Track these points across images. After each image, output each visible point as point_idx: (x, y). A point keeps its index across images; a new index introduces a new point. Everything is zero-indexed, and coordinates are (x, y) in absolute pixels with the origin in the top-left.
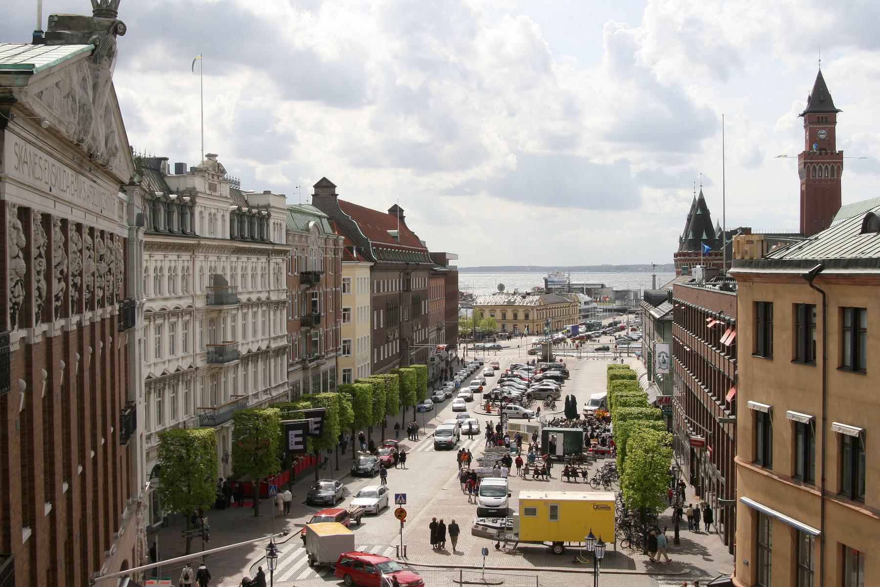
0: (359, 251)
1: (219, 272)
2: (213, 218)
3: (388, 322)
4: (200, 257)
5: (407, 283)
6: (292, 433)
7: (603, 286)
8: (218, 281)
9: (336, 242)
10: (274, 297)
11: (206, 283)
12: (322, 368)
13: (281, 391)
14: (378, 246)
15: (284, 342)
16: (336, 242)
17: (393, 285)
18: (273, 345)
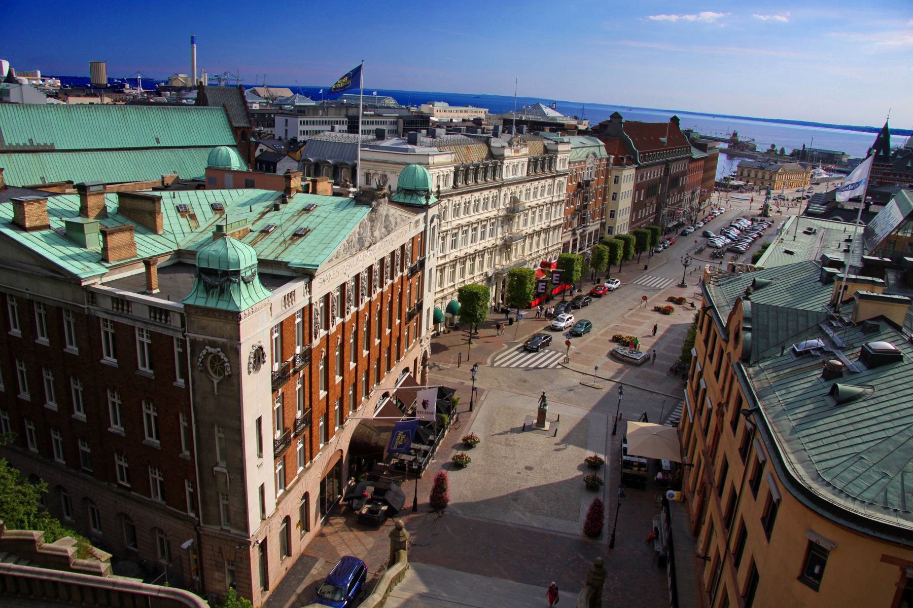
0: (629, 158)
1: (518, 195)
2: (515, 167)
3: (647, 195)
4: (504, 190)
5: (667, 170)
6: (540, 284)
7: (843, 153)
8: (515, 200)
9: (608, 160)
10: (555, 200)
11: (508, 201)
12: (587, 232)
13: (555, 247)
14: (644, 154)
15: (562, 221)
16: (608, 160)
17: (655, 173)
18: (552, 225)
